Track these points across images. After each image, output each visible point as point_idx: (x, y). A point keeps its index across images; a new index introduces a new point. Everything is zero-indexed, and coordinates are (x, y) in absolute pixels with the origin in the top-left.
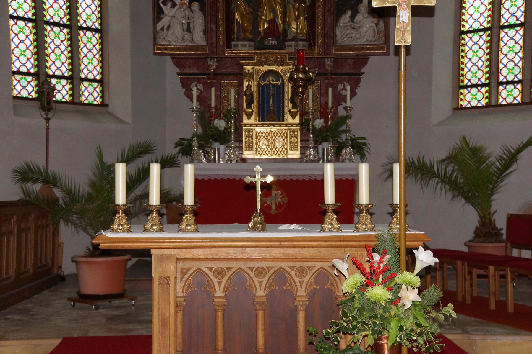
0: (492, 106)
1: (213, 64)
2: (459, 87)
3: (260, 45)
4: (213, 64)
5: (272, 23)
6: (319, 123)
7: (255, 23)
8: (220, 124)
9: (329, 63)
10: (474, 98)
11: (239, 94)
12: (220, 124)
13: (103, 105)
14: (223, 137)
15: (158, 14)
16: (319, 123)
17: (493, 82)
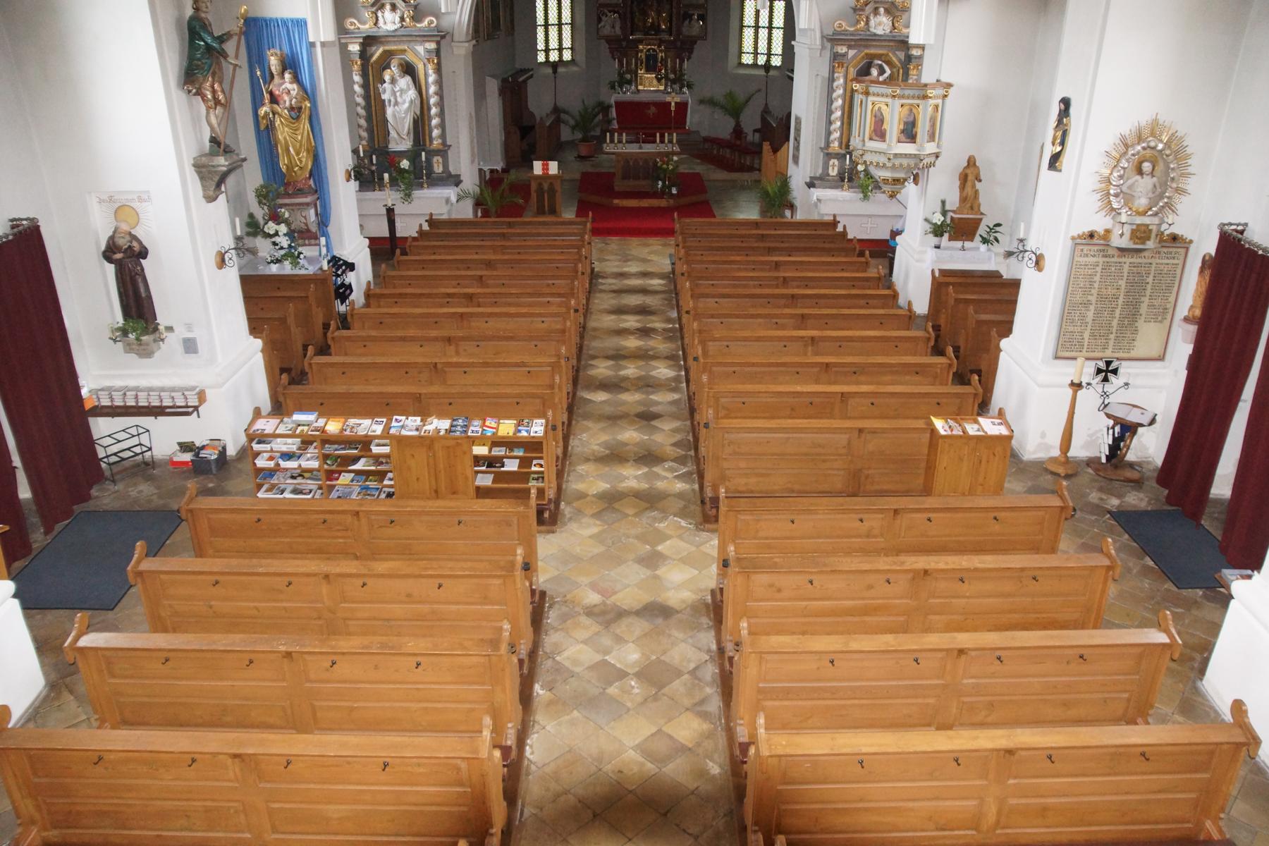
0: (755, 65)
1: (624, 44)
2: (741, 53)
3: (646, 34)
4: (624, 44)
5: (653, 23)
6: (672, 76)
7: (645, 22)
8: (628, 76)
9: (679, 44)
10: (747, 59)
11: (637, 59)
12: (628, 76)
13: (573, 60)
14: (629, 82)
15: (600, 20)
16: (672, 76)
17: (756, 53)
